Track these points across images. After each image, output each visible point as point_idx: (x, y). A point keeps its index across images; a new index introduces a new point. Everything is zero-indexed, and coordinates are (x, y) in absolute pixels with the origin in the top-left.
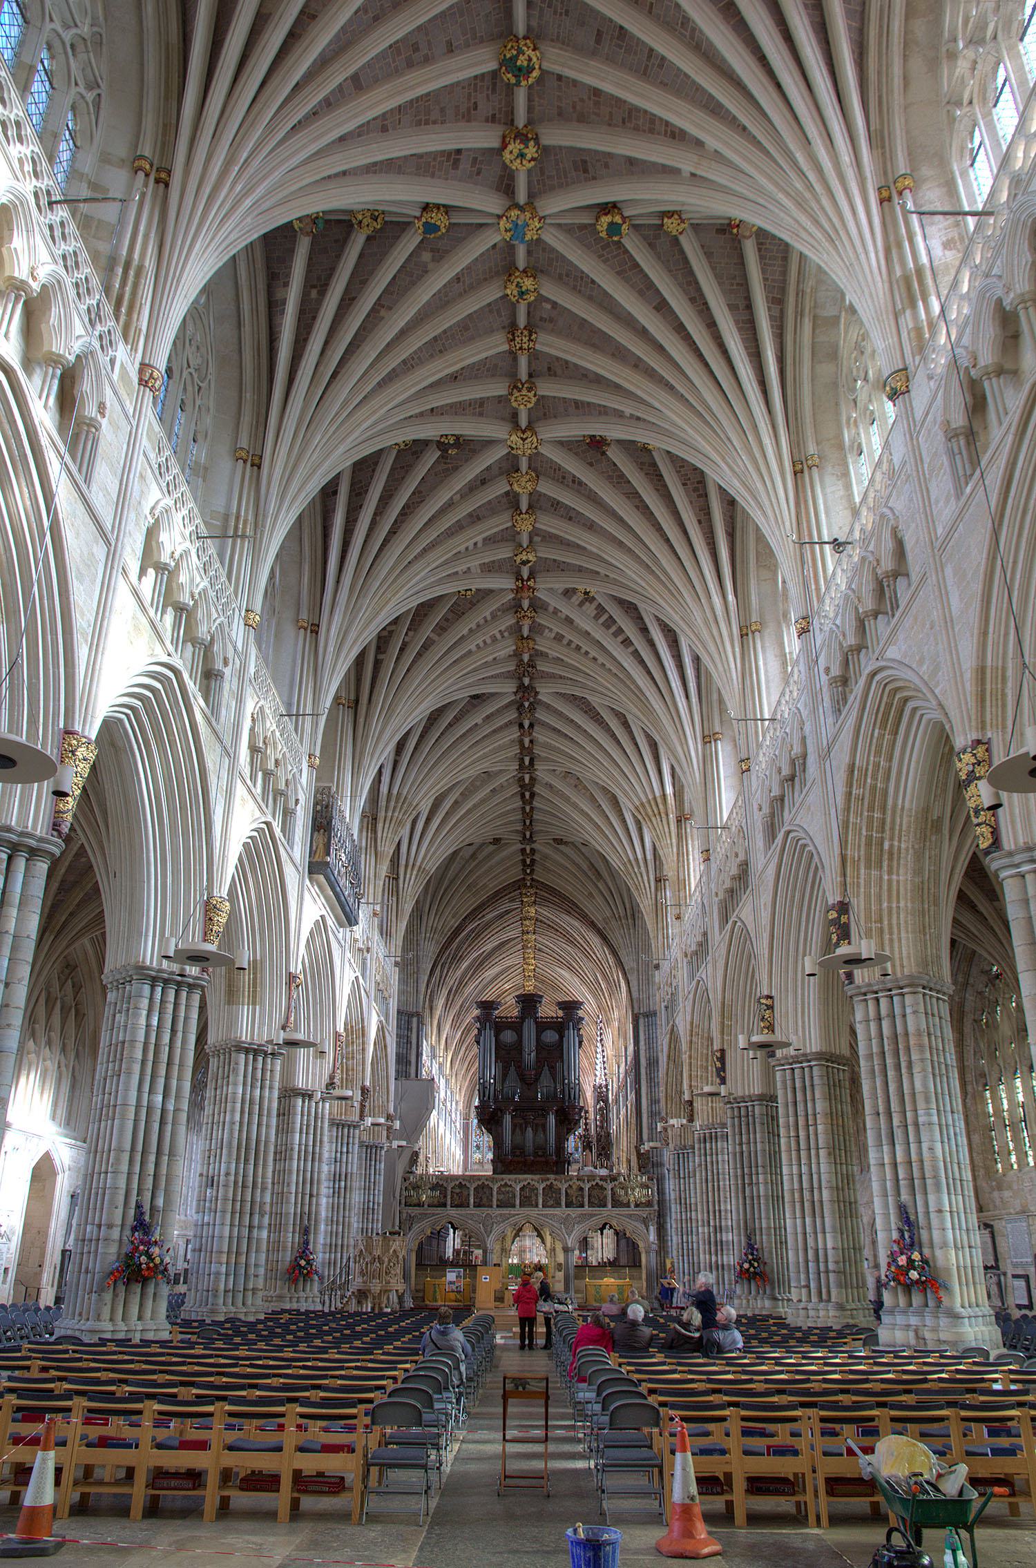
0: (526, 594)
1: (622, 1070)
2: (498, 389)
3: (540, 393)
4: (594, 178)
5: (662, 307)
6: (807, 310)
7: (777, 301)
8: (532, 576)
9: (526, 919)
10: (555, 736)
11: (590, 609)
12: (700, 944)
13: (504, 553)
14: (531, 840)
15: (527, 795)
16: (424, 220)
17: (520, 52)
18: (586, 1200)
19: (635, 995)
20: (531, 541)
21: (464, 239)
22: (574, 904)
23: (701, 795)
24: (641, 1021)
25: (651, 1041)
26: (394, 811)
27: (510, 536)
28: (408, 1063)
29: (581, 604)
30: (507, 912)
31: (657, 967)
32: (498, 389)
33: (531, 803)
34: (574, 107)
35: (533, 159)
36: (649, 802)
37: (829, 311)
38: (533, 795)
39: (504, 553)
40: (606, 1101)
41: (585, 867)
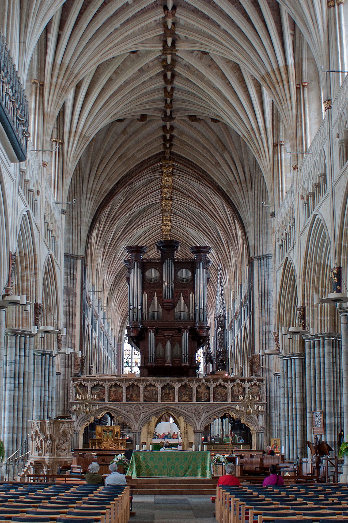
1: (237, 304)
9: (165, 187)
10: (194, 17)
12: (318, 185)
14: (170, 118)
15: (169, 75)
18: (212, 395)
19: (251, 242)
22: (204, 172)
23: (325, 53)
24: (255, 263)
25: (263, 278)
26: (58, 78)
28: (75, 294)
30: (151, 181)
31: (273, 215)
33: (171, 82)
36: (273, 71)
38: (173, 76)
40: (223, 327)
41: (213, 140)
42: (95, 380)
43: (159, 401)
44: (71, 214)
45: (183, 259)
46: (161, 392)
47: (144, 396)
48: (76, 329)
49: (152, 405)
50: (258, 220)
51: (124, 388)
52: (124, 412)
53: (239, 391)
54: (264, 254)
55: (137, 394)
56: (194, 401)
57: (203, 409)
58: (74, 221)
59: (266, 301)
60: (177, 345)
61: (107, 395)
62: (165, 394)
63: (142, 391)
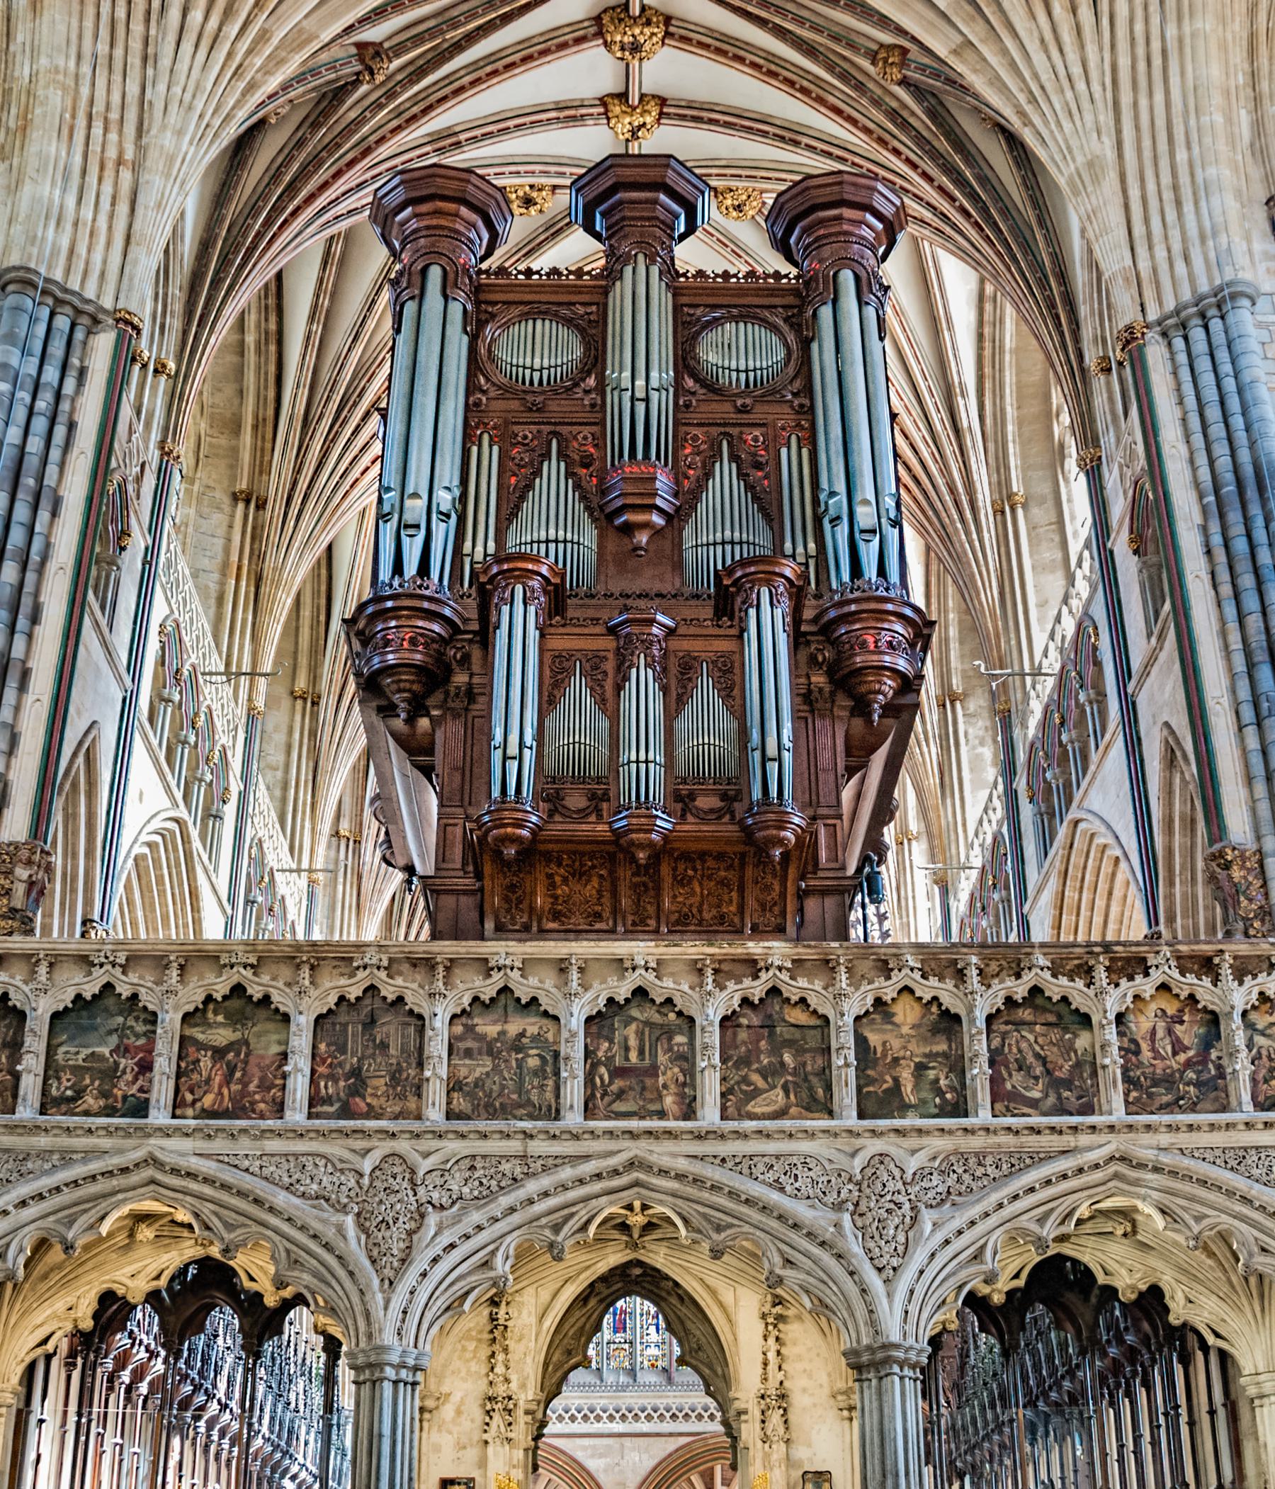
18: (979, 1073)
24: (1155, 354)
42: (85, 961)
43: (573, 1119)
44: (85, 91)
45: (726, 275)
46: (588, 1054)
47: (454, 1086)
48: (29, 699)
49: (514, 1146)
50: (1147, 143)
51: (303, 1023)
52: (281, 1199)
53: (1178, 1047)
54: (1204, 287)
55: (395, 1077)
56: (850, 1119)
57: (921, 1174)
58: (97, 130)
59: (1259, 522)
60: (706, 691)
61: (164, 1063)
62: (617, 1072)
63: (437, 1046)
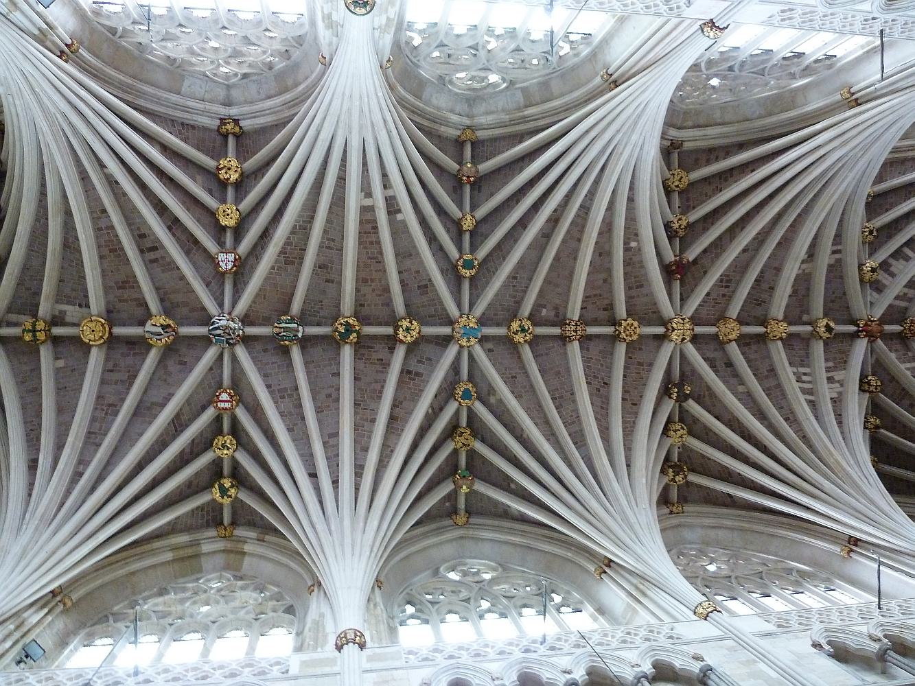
0: (874, 327)
2: (621, 349)
3: (625, 316)
4: (430, 280)
5: (523, 223)
6: (521, 114)
7: (521, 137)
8: (854, 322)
11: (897, 266)
13: (818, 348)
16: (460, 399)
17: (336, 330)
20: (809, 324)
21: (481, 371)
27: (797, 346)
29: (892, 275)
32: (621, 349)
34: (380, 295)
35: (410, 322)
37: (519, 97)
39: (818, 348)
